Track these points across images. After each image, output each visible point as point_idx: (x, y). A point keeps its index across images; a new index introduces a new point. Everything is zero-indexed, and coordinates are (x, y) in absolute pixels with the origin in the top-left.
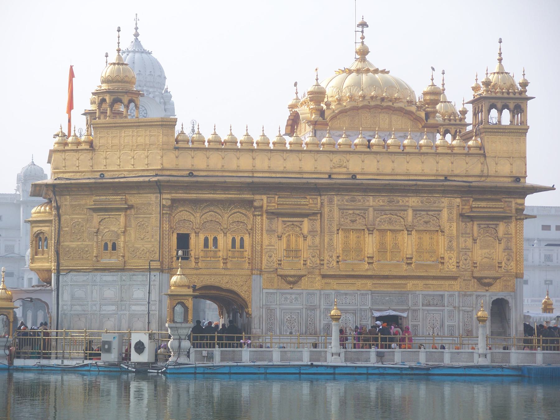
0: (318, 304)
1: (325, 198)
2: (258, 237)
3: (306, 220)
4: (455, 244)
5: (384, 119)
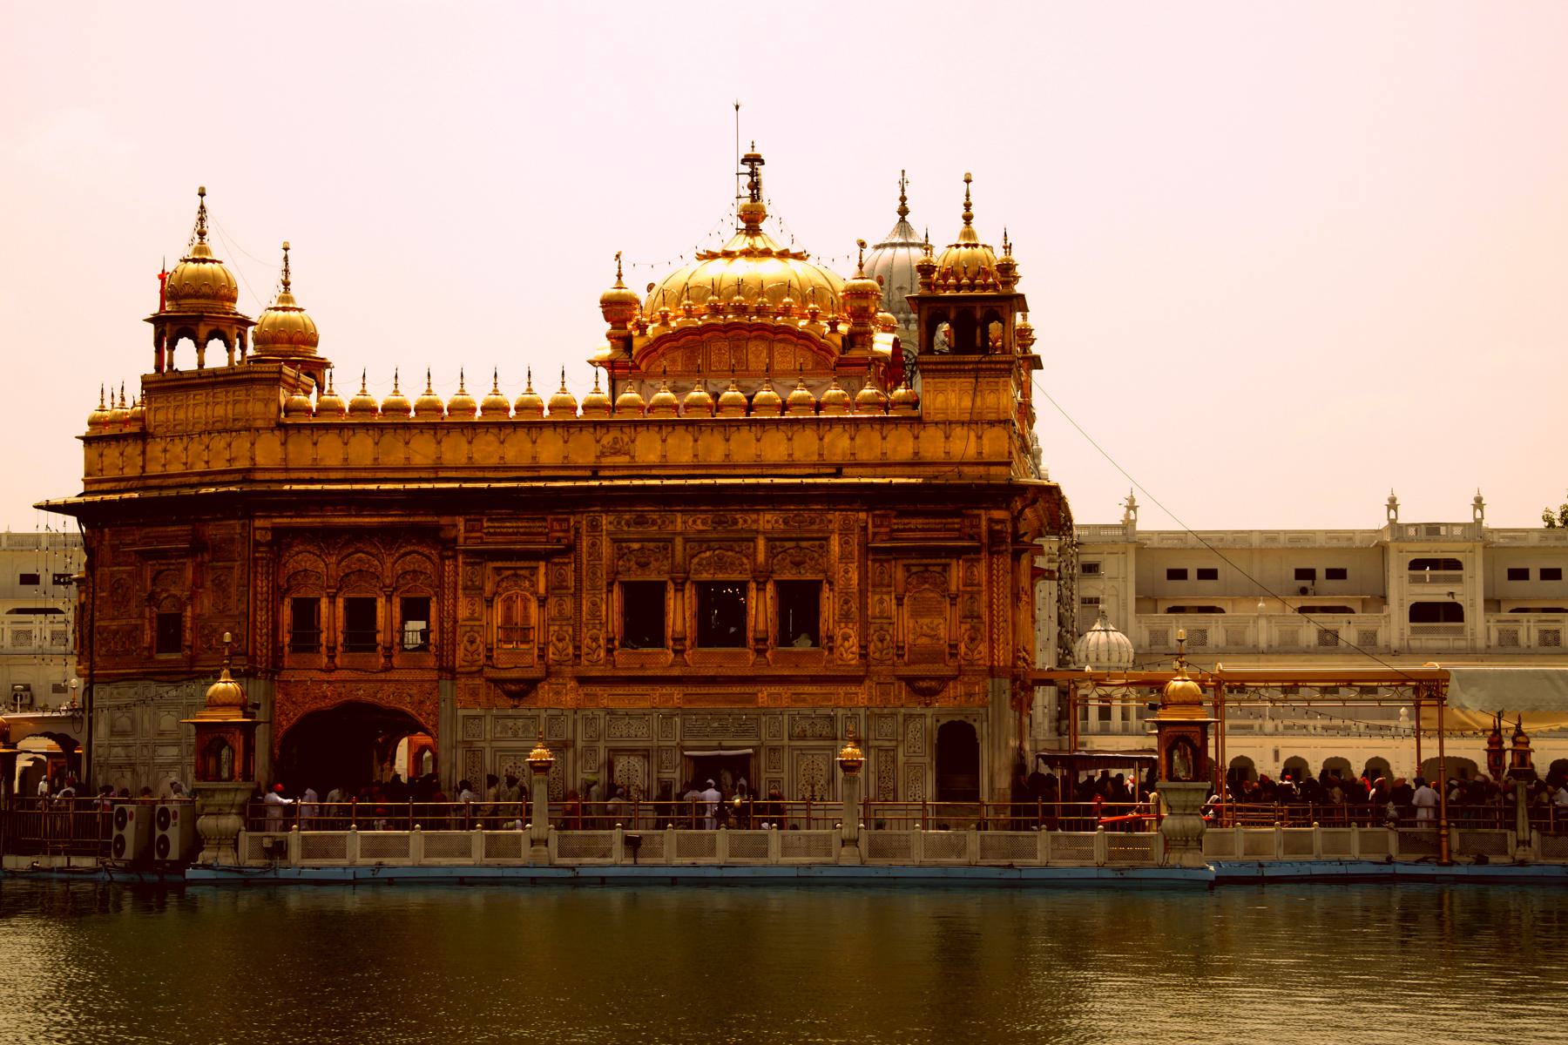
0: (570, 736)
2: (448, 602)
3: (542, 565)
5: (756, 354)
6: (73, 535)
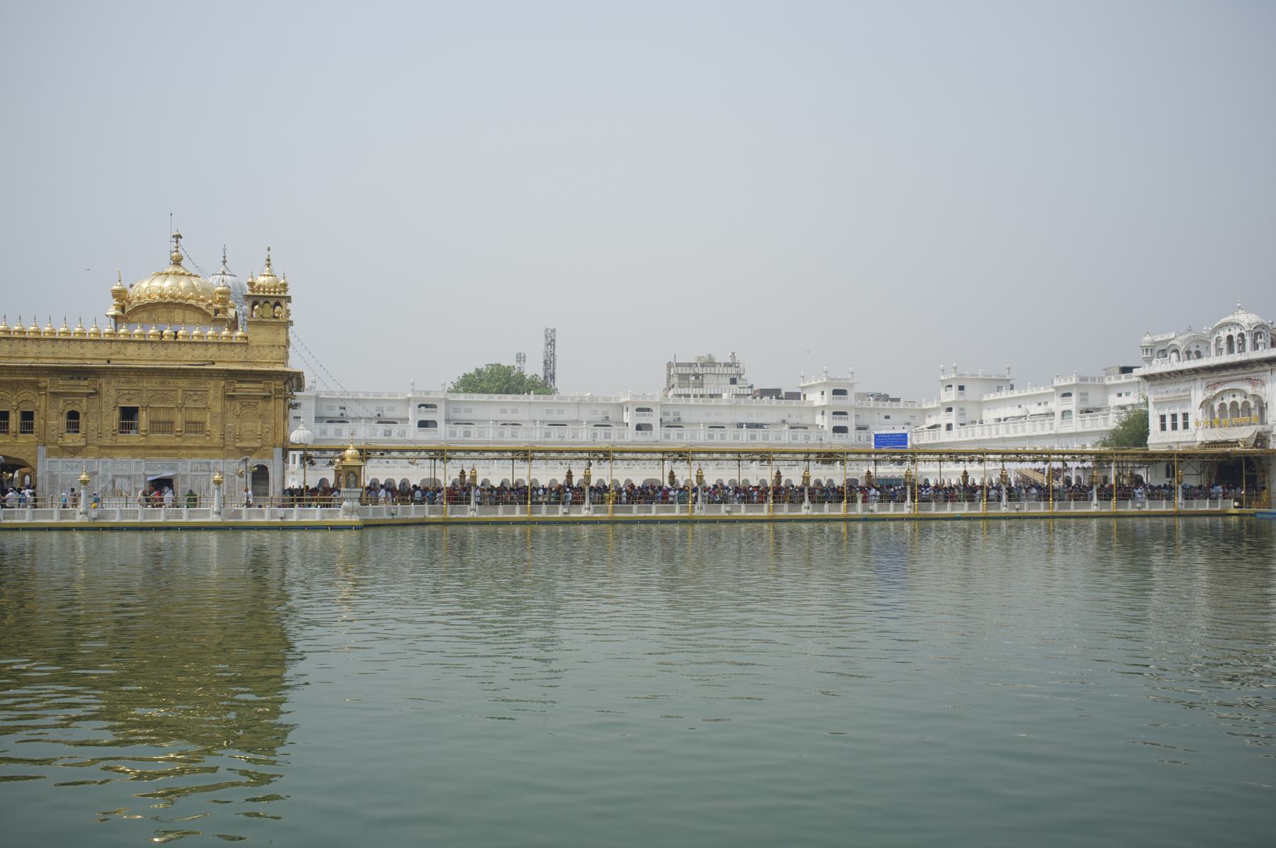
3: (85, 400)
5: (178, 315)
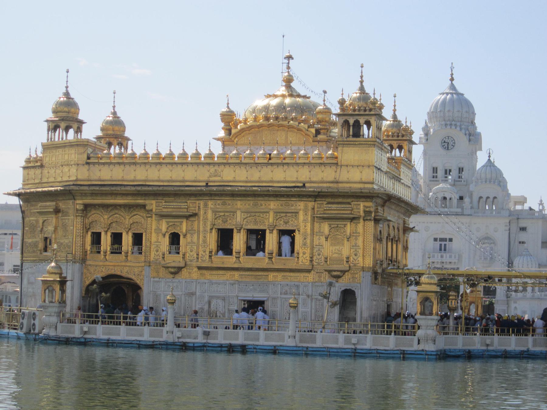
1: (202, 203)
3: (185, 221)
4: (308, 241)
5: (281, 136)
6: (16, 205)
